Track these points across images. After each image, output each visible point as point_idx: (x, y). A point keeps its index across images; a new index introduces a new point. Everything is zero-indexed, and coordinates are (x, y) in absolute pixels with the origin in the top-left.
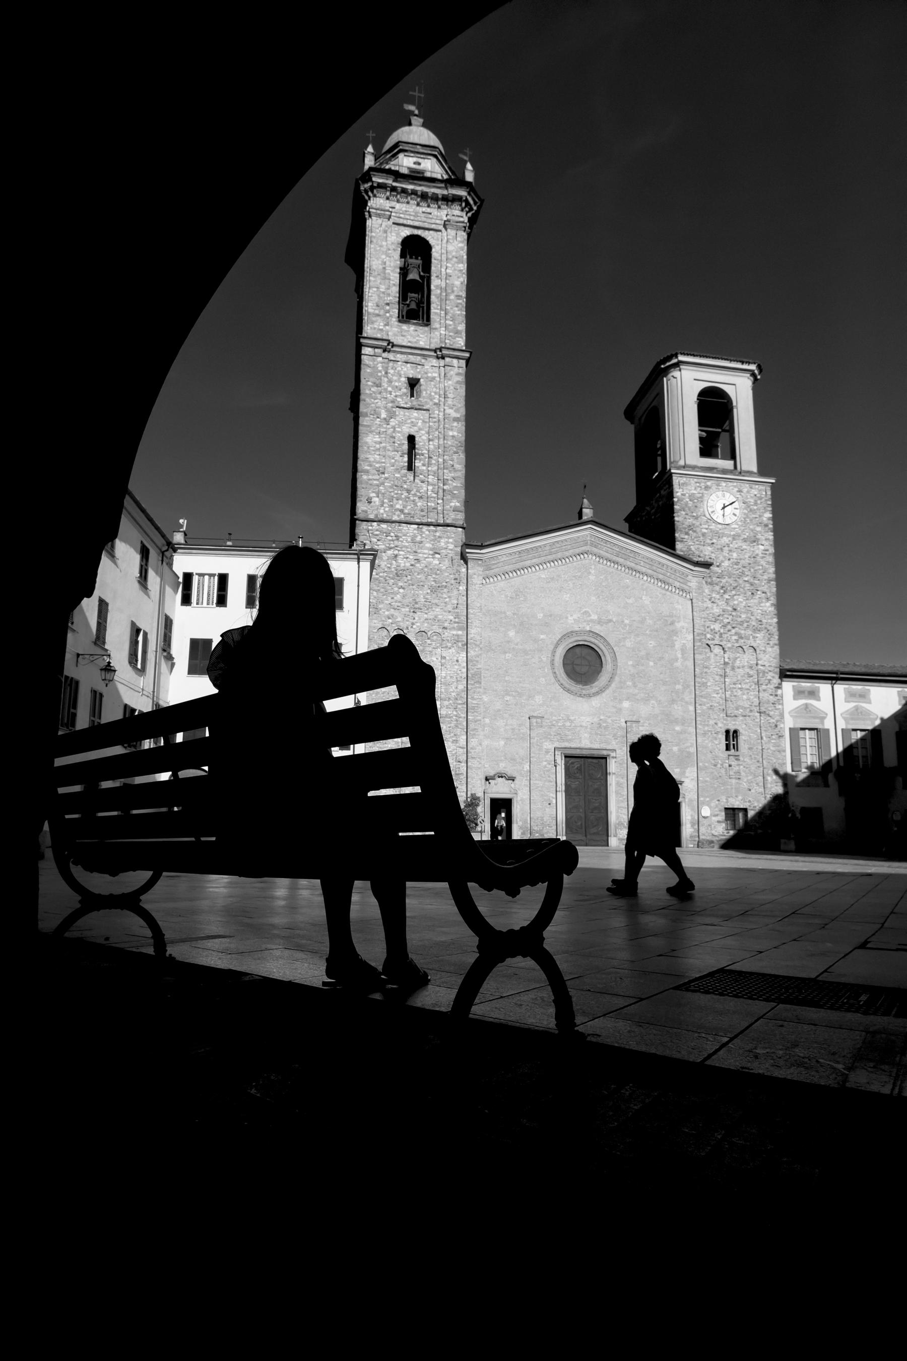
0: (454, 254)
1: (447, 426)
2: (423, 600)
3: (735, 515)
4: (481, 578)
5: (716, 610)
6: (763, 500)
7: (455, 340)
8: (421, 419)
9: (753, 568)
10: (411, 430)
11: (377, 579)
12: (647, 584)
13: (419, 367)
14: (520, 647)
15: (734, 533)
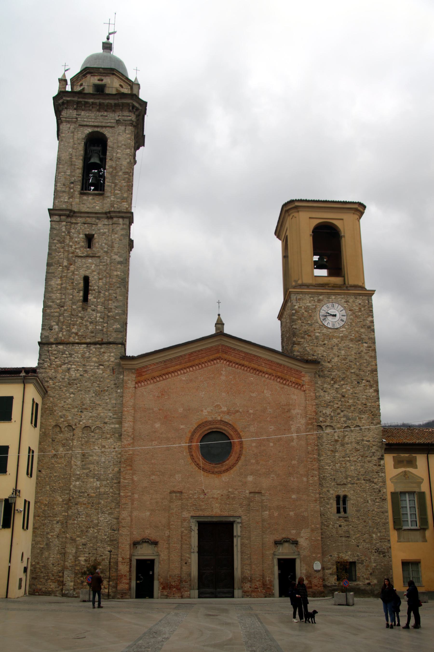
0: (123, 142)
1: (113, 268)
2: (89, 402)
3: (342, 320)
4: (134, 383)
5: (328, 398)
6: (366, 307)
7: (120, 205)
8: (94, 264)
9: (358, 362)
10: (87, 272)
11: (54, 388)
12: (268, 381)
13: (94, 226)
14: (164, 436)
15: (342, 335)
